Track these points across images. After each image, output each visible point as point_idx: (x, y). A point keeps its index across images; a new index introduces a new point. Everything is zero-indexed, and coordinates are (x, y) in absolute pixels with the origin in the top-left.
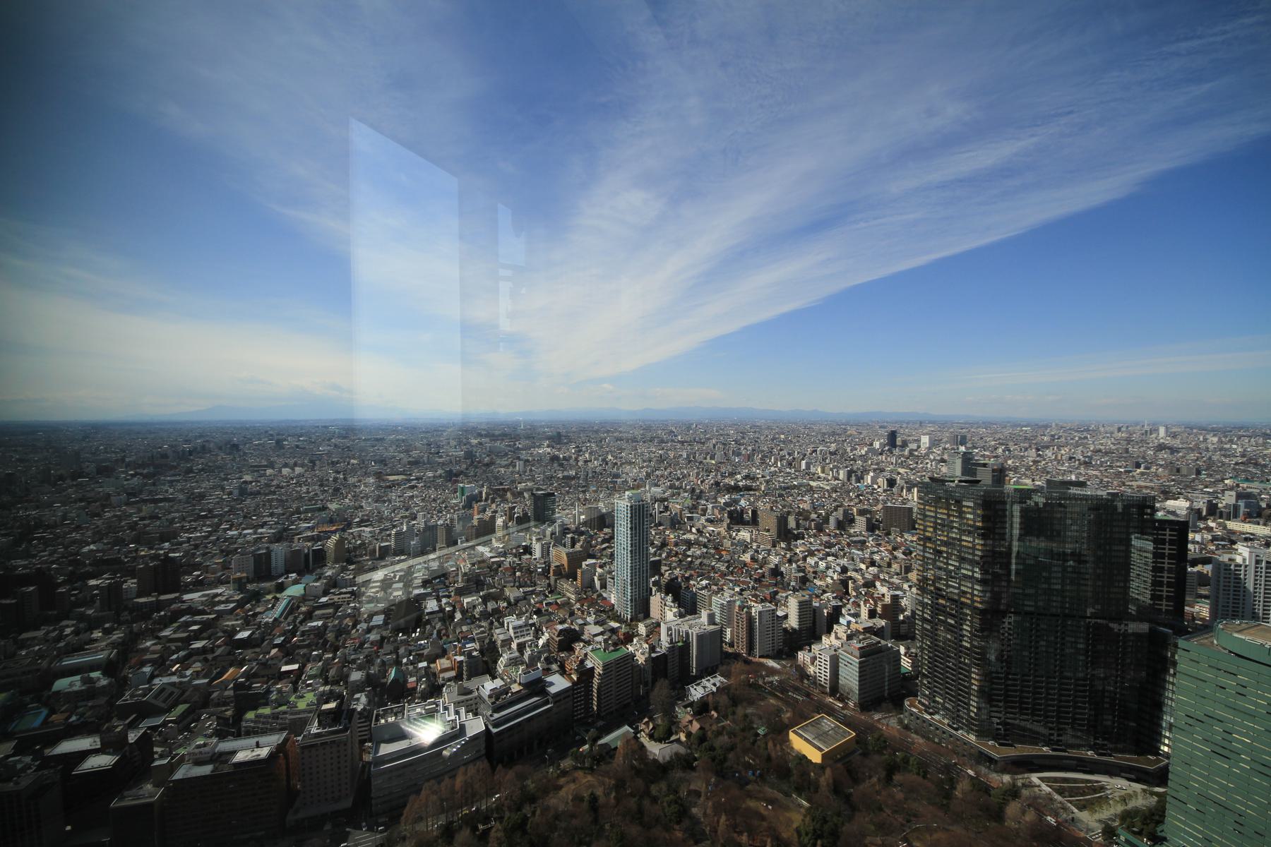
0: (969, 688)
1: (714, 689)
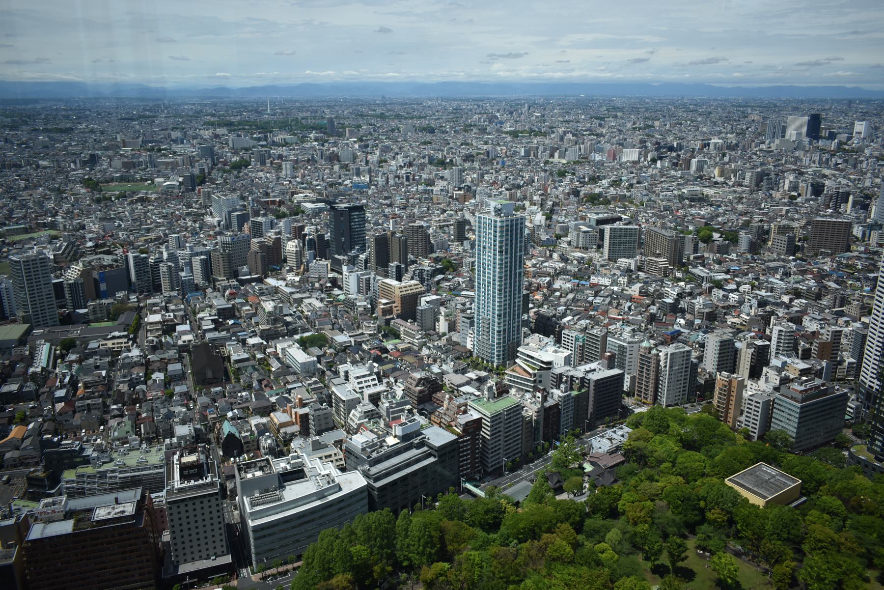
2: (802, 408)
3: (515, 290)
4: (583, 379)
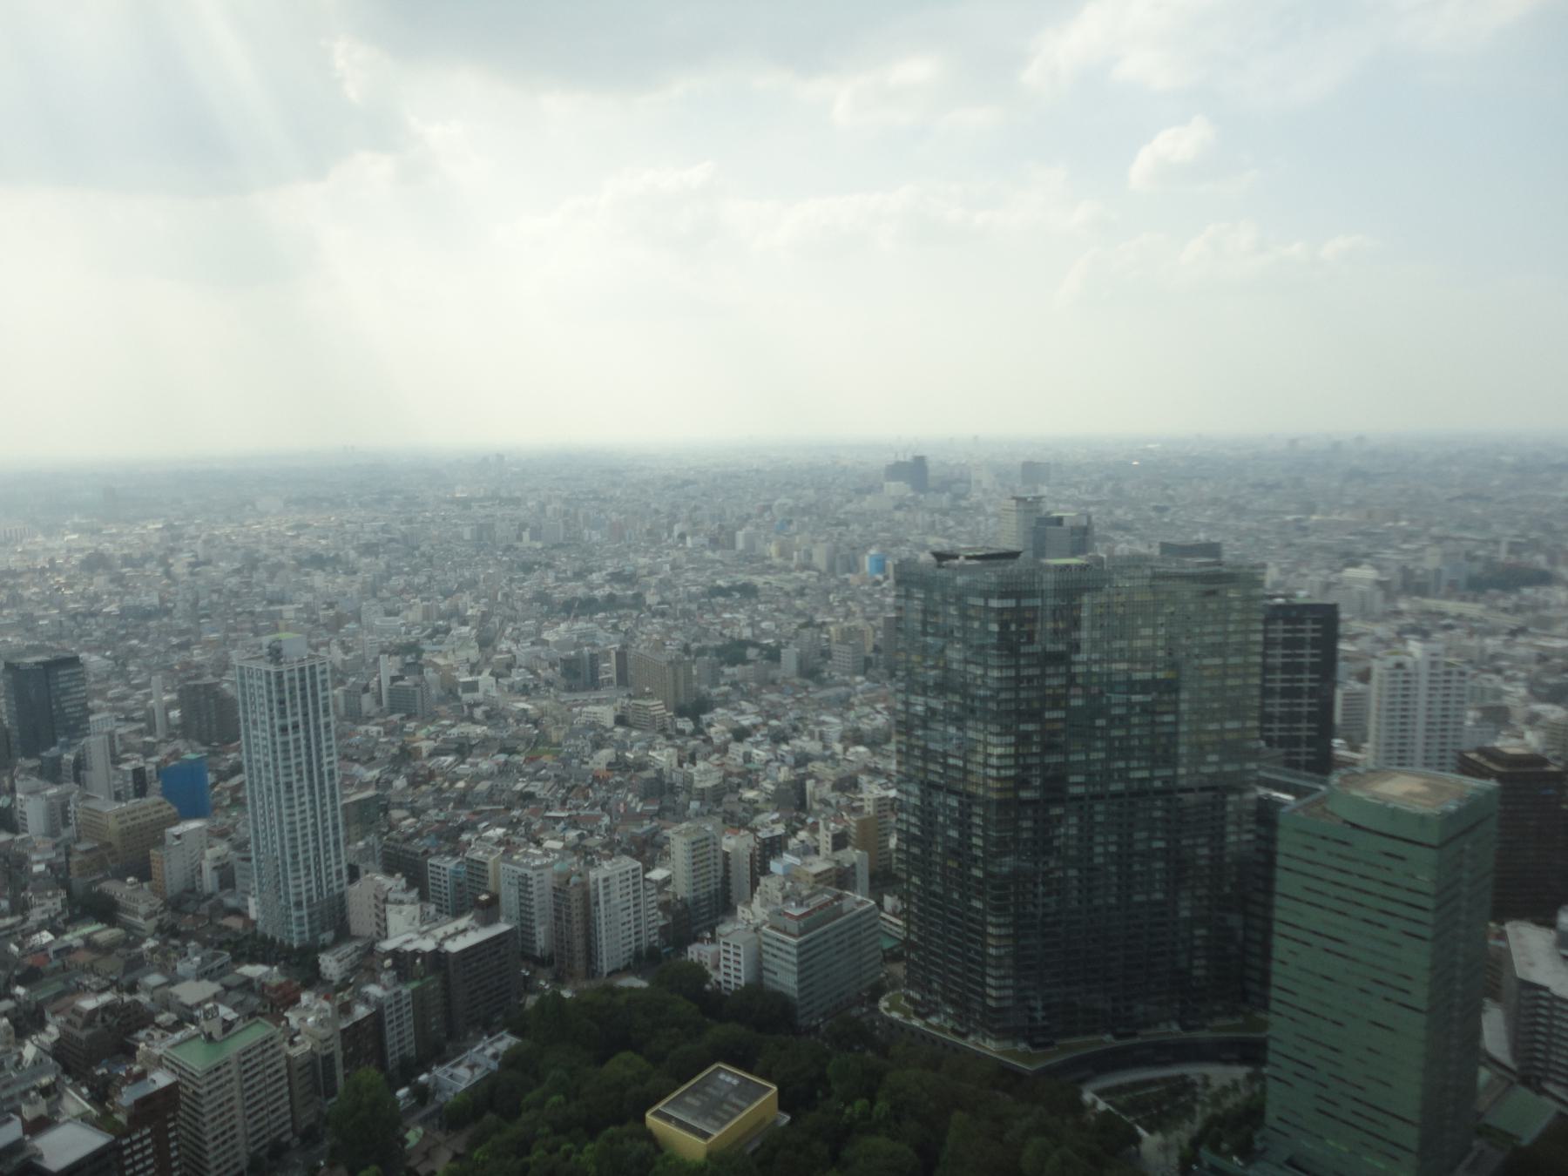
0: (983, 954)
1: (494, 1065)
2: (799, 945)
3: (322, 798)
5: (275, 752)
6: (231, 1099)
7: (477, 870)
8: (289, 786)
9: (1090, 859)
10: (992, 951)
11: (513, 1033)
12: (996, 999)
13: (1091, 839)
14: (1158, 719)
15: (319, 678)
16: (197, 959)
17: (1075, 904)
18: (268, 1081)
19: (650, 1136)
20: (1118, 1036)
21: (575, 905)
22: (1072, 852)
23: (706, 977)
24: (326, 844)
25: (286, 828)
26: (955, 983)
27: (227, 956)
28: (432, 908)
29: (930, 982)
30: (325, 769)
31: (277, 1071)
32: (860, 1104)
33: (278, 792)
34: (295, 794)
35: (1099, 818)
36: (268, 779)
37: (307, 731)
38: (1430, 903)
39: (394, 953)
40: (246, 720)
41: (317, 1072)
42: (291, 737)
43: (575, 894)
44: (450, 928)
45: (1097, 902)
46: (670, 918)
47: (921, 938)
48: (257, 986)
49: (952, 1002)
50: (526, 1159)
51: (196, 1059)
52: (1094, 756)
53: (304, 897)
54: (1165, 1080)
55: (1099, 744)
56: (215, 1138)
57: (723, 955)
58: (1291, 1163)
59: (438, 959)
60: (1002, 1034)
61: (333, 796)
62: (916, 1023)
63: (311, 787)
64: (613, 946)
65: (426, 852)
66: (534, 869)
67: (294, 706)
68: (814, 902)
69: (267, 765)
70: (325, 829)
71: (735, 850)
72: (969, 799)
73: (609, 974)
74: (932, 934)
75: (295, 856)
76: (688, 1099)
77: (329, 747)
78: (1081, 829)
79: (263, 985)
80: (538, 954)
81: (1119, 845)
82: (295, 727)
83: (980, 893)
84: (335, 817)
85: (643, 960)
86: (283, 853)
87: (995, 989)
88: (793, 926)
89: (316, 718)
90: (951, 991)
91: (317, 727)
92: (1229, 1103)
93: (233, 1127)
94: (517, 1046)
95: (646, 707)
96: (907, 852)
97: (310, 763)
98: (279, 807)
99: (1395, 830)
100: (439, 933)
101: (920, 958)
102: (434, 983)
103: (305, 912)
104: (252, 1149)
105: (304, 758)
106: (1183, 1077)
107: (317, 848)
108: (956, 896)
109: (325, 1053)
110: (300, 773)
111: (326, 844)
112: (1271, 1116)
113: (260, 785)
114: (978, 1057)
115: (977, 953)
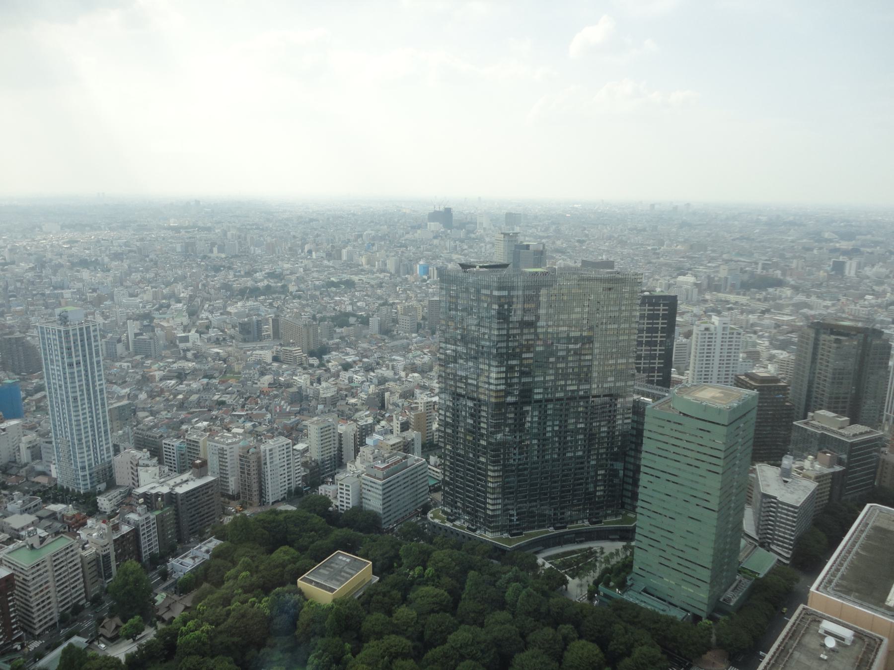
0: (486, 487)
1: (207, 557)
2: (384, 485)
3: (96, 405)
4: (170, 494)
5: (65, 378)
6: (47, 582)
7: (193, 446)
8: (75, 399)
9: (545, 434)
10: (490, 485)
11: (217, 538)
12: (492, 510)
13: (545, 423)
14: (582, 358)
15: (92, 334)
16: (20, 501)
17: (535, 458)
18: (70, 571)
19: (300, 592)
20: (556, 528)
21: (253, 467)
22: (535, 431)
23: (329, 503)
24: (99, 433)
25: (74, 423)
26: (470, 503)
27: (39, 499)
28: (166, 469)
29: (456, 502)
30: (98, 388)
31: (75, 565)
32: (418, 569)
33: (68, 402)
34: (79, 403)
35: (549, 412)
36: (61, 395)
37: (86, 366)
38: (722, 455)
39: (145, 495)
40: (46, 359)
41: (101, 564)
42: (75, 370)
43: (253, 458)
44: (178, 480)
45: (547, 457)
46: (308, 471)
47: (451, 479)
48: (59, 516)
49: (469, 513)
50: (228, 608)
51: (24, 560)
52: (548, 378)
53: (87, 464)
54: (581, 550)
55: (551, 372)
56: (38, 605)
57: (339, 491)
58: (645, 591)
59: (171, 498)
60: (495, 529)
61: (103, 405)
62: (448, 524)
63: (89, 399)
64: (275, 488)
65: (161, 436)
66: (228, 445)
67: (77, 351)
68: (391, 461)
69: (60, 386)
70: (98, 423)
71: (346, 432)
72: (479, 402)
73: (273, 503)
74: (457, 476)
75: (80, 440)
76: (321, 571)
77: (100, 375)
78: (540, 418)
79: (63, 516)
80: (231, 493)
81: (560, 427)
82: (78, 363)
83: (484, 453)
84: (104, 417)
85: (293, 495)
86: (73, 439)
87: (493, 505)
88: (380, 474)
89: (91, 358)
90: (468, 507)
91: (92, 364)
92: (614, 561)
93: (49, 598)
94: (221, 545)
95: (291, 351)
96: (444, 432)
97: (88, 385)
98: (69, 411)
99: (705, 419)
100: (172, 483)
101: (451, 489)
102: (169, 511)
103: (87, 473)
104: (61, 610)
105: (84, 382)
106: (590, 548)
107: (94, 435)
108: (471, 455)
109: (104, 553)
110: (82, 391)
111: (99, 433)
112: (636, 568)
113: (56, 398)
114: (482, 542)
115: (482, 486)
